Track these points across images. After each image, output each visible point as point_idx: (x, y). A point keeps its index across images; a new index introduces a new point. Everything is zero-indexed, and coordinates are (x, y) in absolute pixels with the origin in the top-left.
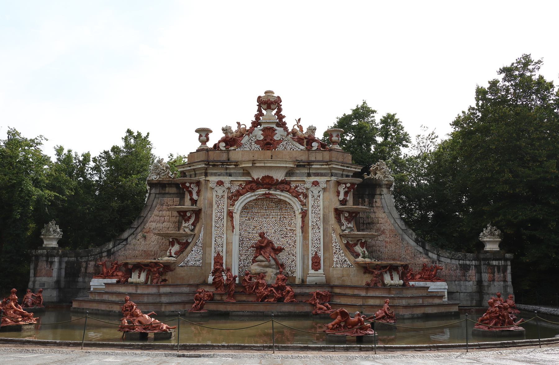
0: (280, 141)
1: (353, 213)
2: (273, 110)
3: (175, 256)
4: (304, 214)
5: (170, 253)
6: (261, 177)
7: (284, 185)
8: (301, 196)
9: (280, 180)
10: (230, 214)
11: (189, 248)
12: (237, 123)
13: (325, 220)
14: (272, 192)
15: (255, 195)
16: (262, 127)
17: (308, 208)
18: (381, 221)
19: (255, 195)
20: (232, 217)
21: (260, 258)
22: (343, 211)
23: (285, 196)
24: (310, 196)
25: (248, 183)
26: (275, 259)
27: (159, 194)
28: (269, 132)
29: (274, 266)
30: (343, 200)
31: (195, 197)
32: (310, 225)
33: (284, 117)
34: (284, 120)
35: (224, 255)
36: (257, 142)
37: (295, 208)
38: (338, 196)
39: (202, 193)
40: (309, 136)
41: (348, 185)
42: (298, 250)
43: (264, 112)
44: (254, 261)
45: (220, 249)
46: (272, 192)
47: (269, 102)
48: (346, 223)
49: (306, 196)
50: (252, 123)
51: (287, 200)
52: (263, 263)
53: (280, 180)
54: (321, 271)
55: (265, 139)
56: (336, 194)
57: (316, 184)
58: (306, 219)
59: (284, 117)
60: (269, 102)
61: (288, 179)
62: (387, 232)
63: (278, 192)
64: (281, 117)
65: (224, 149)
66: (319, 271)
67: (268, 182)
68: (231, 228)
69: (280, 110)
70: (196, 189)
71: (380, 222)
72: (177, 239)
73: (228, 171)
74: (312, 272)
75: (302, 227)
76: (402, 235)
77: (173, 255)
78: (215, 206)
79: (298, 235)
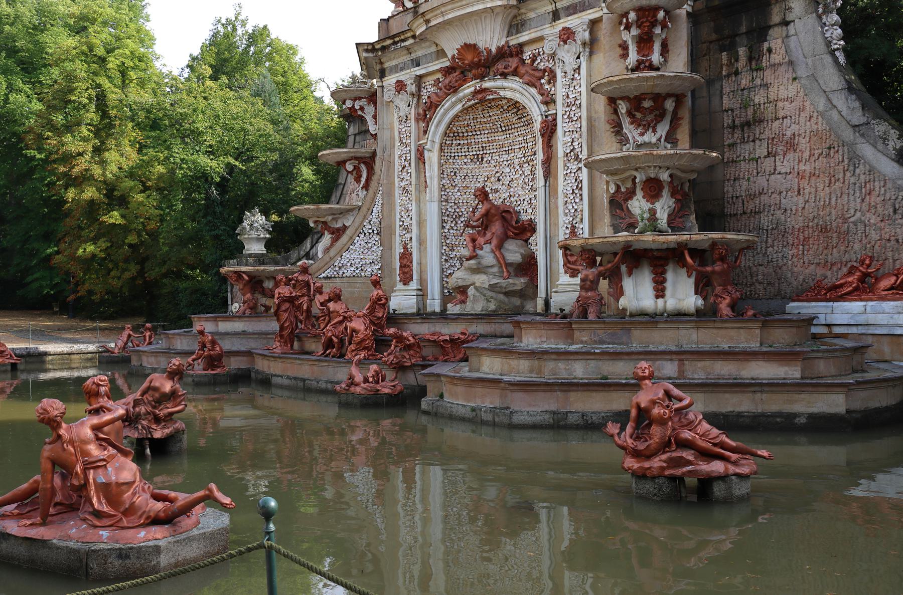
6: (456, 52)
7: (506, 60)
9: (494, 50)
14: (487, 84)
15: (460, 100)
18: (785, 108)
19: (460, 100)
23: (512, 88)
24: (559, 74)
25: (447, 71)
27: (359, 134)
29: (495, 270)
32: (560, 153)
38: (625, 56)
46: (487, 84)
48: (636, 133)
49: (553, 78)
53: (494, 50)
56: (620, 51)
62: (803, 143)
63: (500, 82)
71: (781, 114)
76: (851, 146)
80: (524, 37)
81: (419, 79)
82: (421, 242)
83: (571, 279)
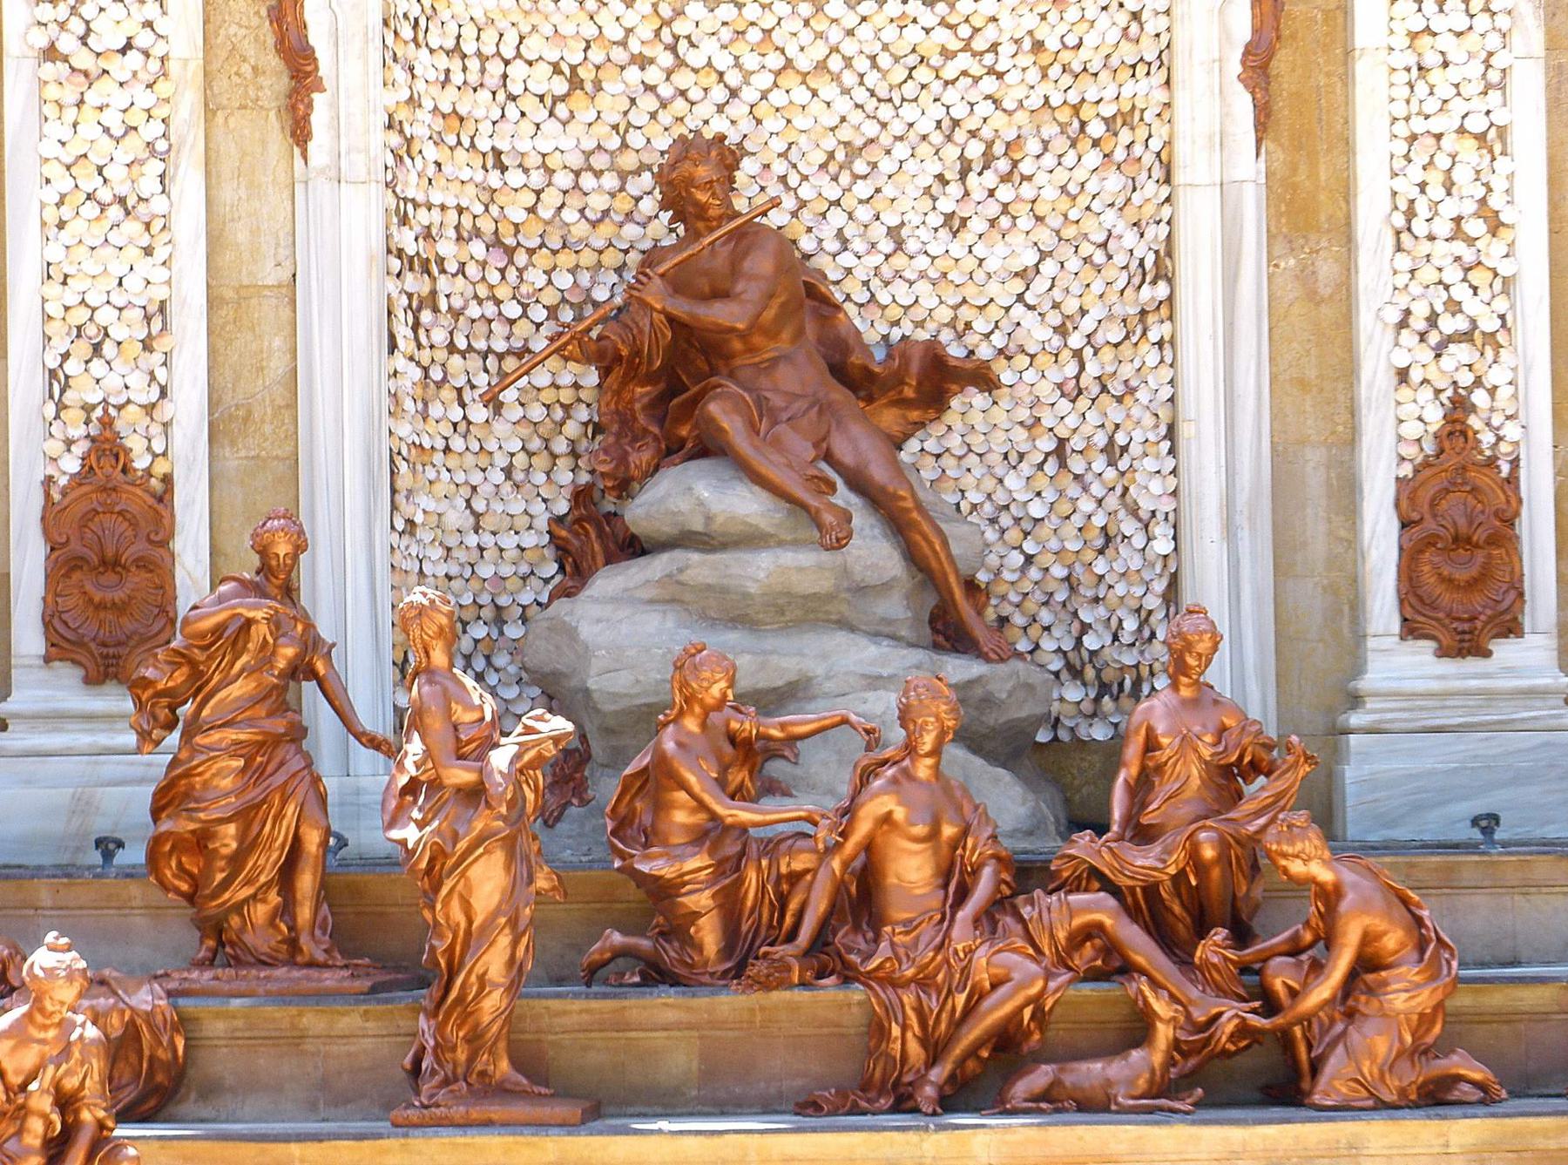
26: (899, 520)
29: (894, 607)
42: (1219, 360)
44: (593, 537)
45: (116, 380)
52: (759, 570)
54: (1526, 658)
66: (1505, 651)
68: (276, 81)
74: (1400, 666)
75: (1258, 65)
79: (1193, 166)
82: (255, 420)
83: (1449, 666)
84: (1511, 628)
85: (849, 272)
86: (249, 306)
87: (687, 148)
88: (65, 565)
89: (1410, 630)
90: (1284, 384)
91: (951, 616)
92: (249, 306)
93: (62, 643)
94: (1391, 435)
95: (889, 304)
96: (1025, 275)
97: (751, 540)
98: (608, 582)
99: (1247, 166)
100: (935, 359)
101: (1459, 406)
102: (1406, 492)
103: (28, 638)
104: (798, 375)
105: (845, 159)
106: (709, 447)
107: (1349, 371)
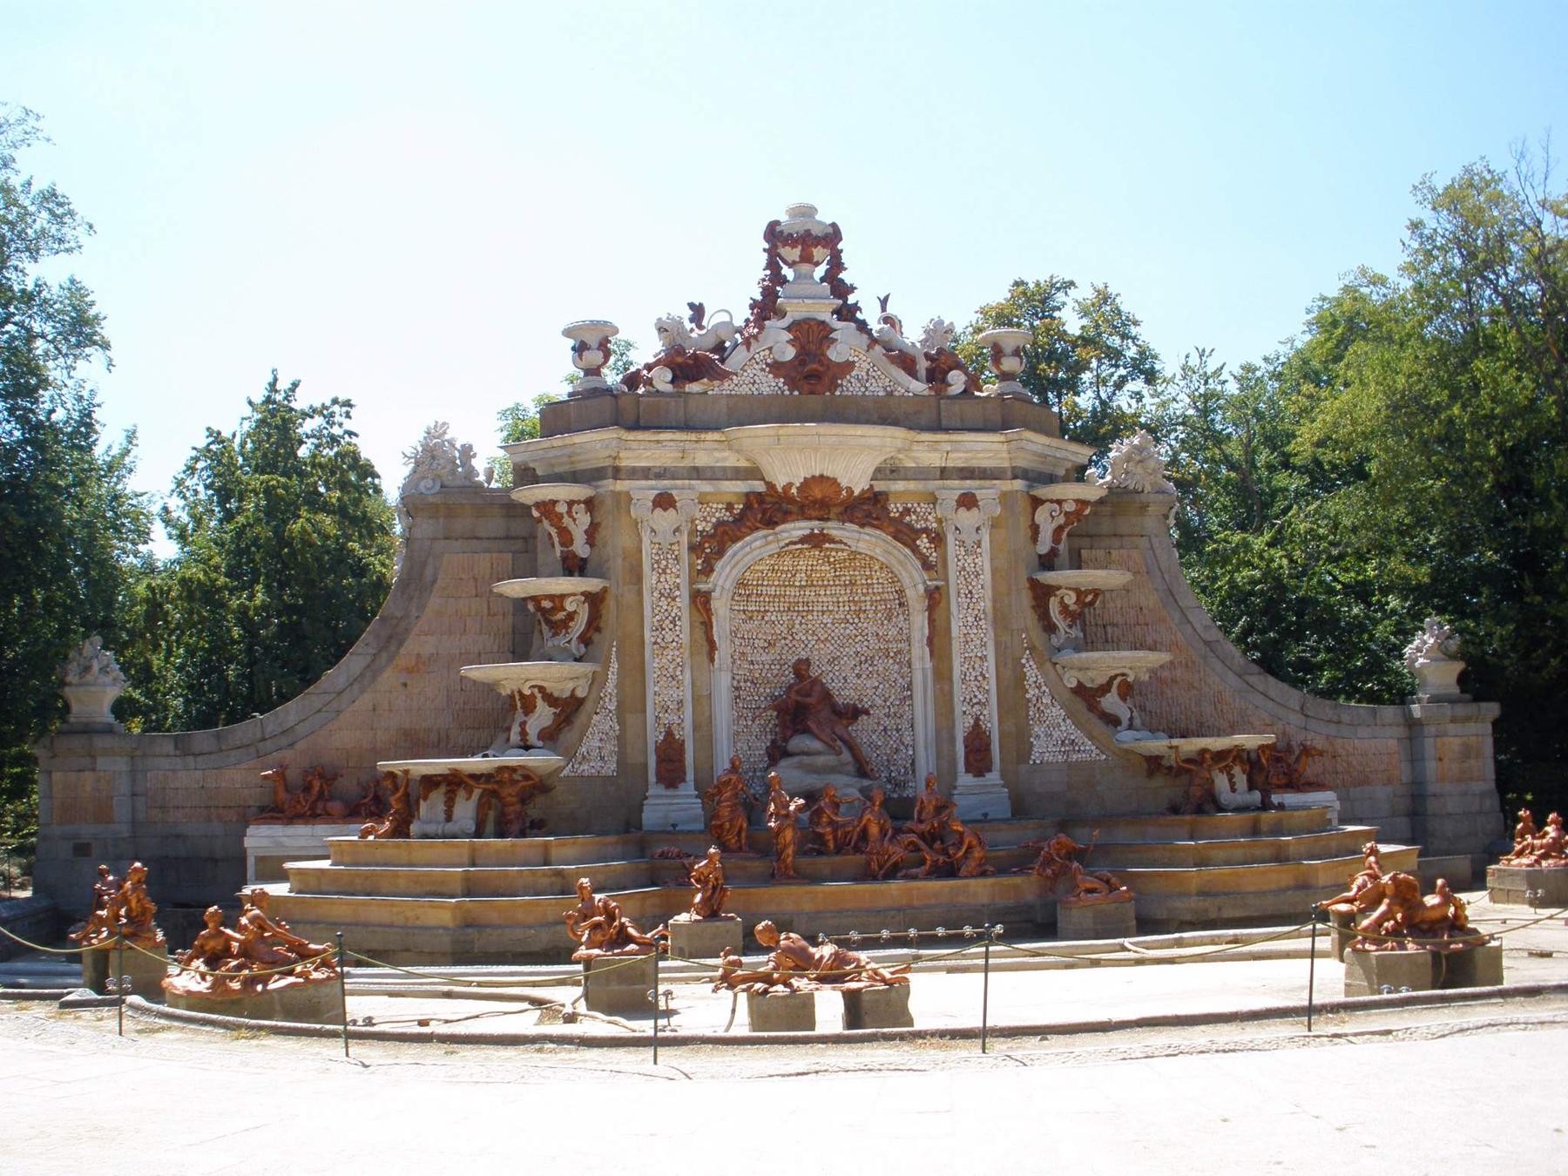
0: (849, 366)
1: (1087, 592)
2: (817, 264)
3: (540, 744)
4: (935, 598)
5: (523, 733)
8: (923, 543)
10: (701, 601)
11: (581, 719)
12: (691, 306)
13: (1001, 620)
16: (786, 322)
17: (946, 580)
20: (708, 611)
21: (799, 742)
22: (1059, 588)
24: (950, 539)
28: (811, 336)
29: (851, 768)
30: (1048, 554)
31: (581, 548)
33: (852, 289)
34: (851, 299)
35: (686, 733)
36: (776, 368)
37: (906, 581)
39: (603, 534)
40: (940, 351)
41: (1070, 507)
43: (788, 272)
44: (777, 753)
47: (802, 243)
49: (938, 539)
50: (752, 307)
51: (878, 552)
52: (820, 760)
53: (856, 493)
54: (993, 777)
55: (801, 359)
57: (968, 501)
58: (939, 614)
59: (852, 289)
60: (802, 243)
61: (880, 486)
64: (841, 289)
65: (669, 388)
66: (988, 776)
67: (819, 501)
68: (706, 648)
69: (836, 265)
70: (584, 519)
72: (541, 689)
73: (687, 463)
74: (965, 779)
77: (532, 738)
78: (650, 579)
79: (917, 665)
80: (899, 486)
81: (703, 500)
82: (703, 726)
84: (990, 770)
85: (834, 686)
86: (702, 700)
87: (799, 661)
88: (660, 761)
89: (967, 771)
90: (938, 715)
91: (862, 770)
92: (702, 700)
93: (660, 779)
94: (962, 726)
95: (845, 694)
96: (876, 688)
97: (819, 753)
98: (783, 763)
99: (929, 665)
100: (855, 706)
101: (977, 719)
102: (966, 739)
103: (652, 778)
104: (825, 714)
105: (833, 661)
106: (806, 731)
107: (952, 711)
